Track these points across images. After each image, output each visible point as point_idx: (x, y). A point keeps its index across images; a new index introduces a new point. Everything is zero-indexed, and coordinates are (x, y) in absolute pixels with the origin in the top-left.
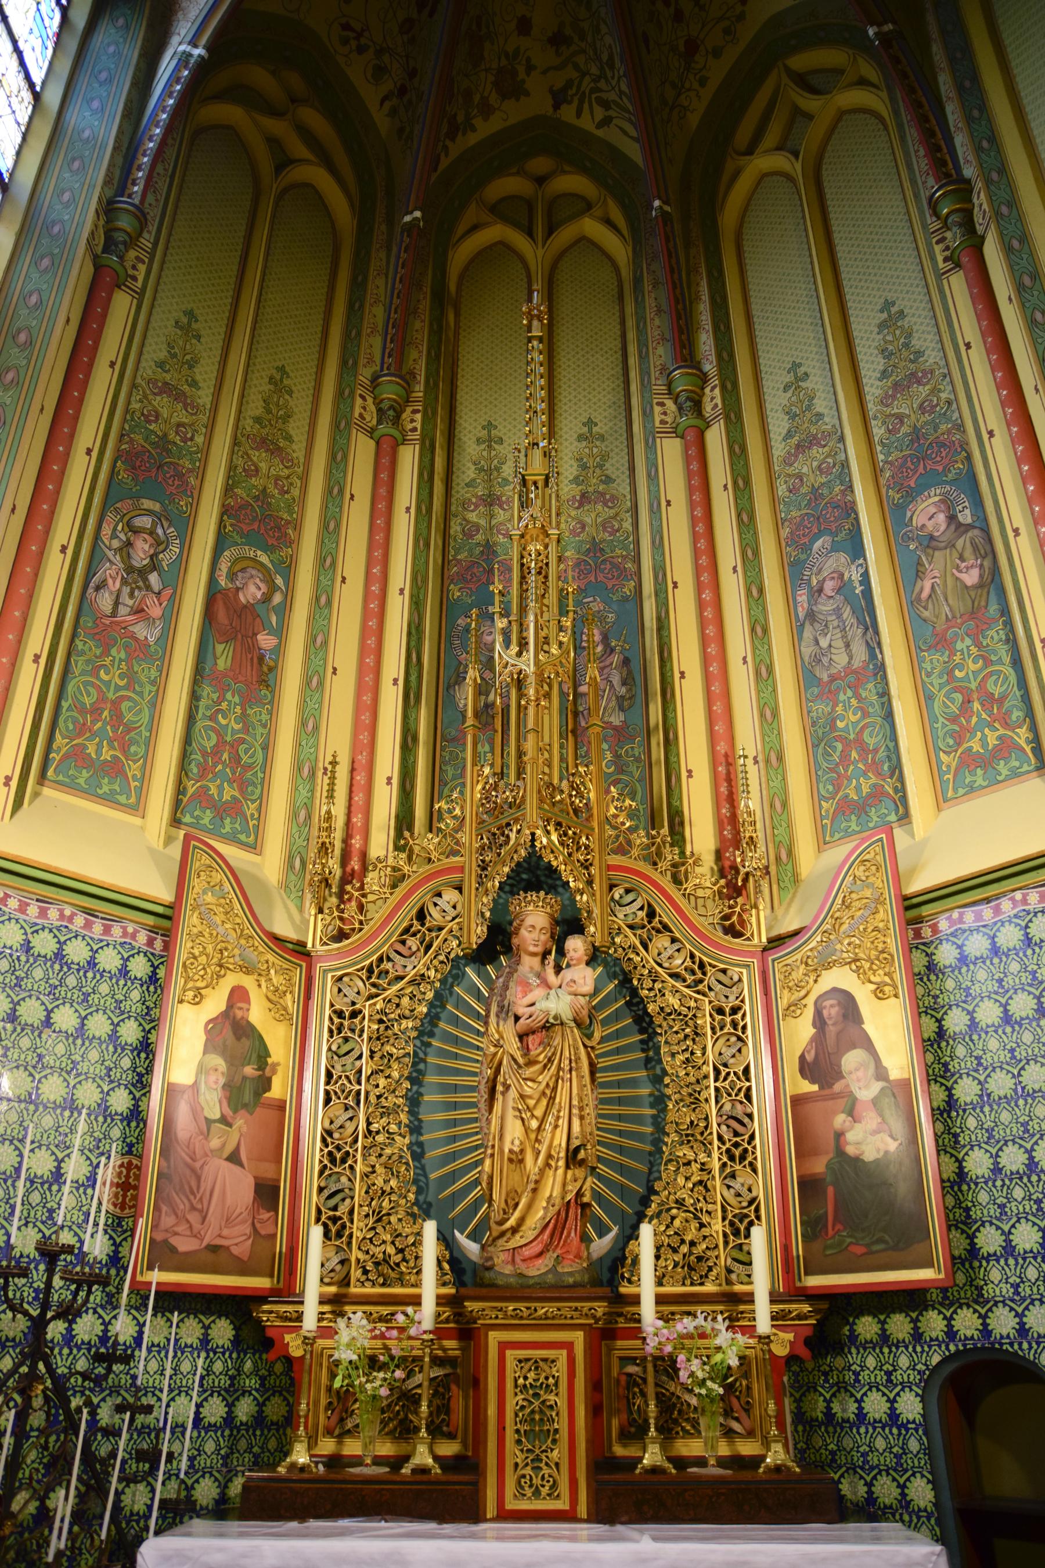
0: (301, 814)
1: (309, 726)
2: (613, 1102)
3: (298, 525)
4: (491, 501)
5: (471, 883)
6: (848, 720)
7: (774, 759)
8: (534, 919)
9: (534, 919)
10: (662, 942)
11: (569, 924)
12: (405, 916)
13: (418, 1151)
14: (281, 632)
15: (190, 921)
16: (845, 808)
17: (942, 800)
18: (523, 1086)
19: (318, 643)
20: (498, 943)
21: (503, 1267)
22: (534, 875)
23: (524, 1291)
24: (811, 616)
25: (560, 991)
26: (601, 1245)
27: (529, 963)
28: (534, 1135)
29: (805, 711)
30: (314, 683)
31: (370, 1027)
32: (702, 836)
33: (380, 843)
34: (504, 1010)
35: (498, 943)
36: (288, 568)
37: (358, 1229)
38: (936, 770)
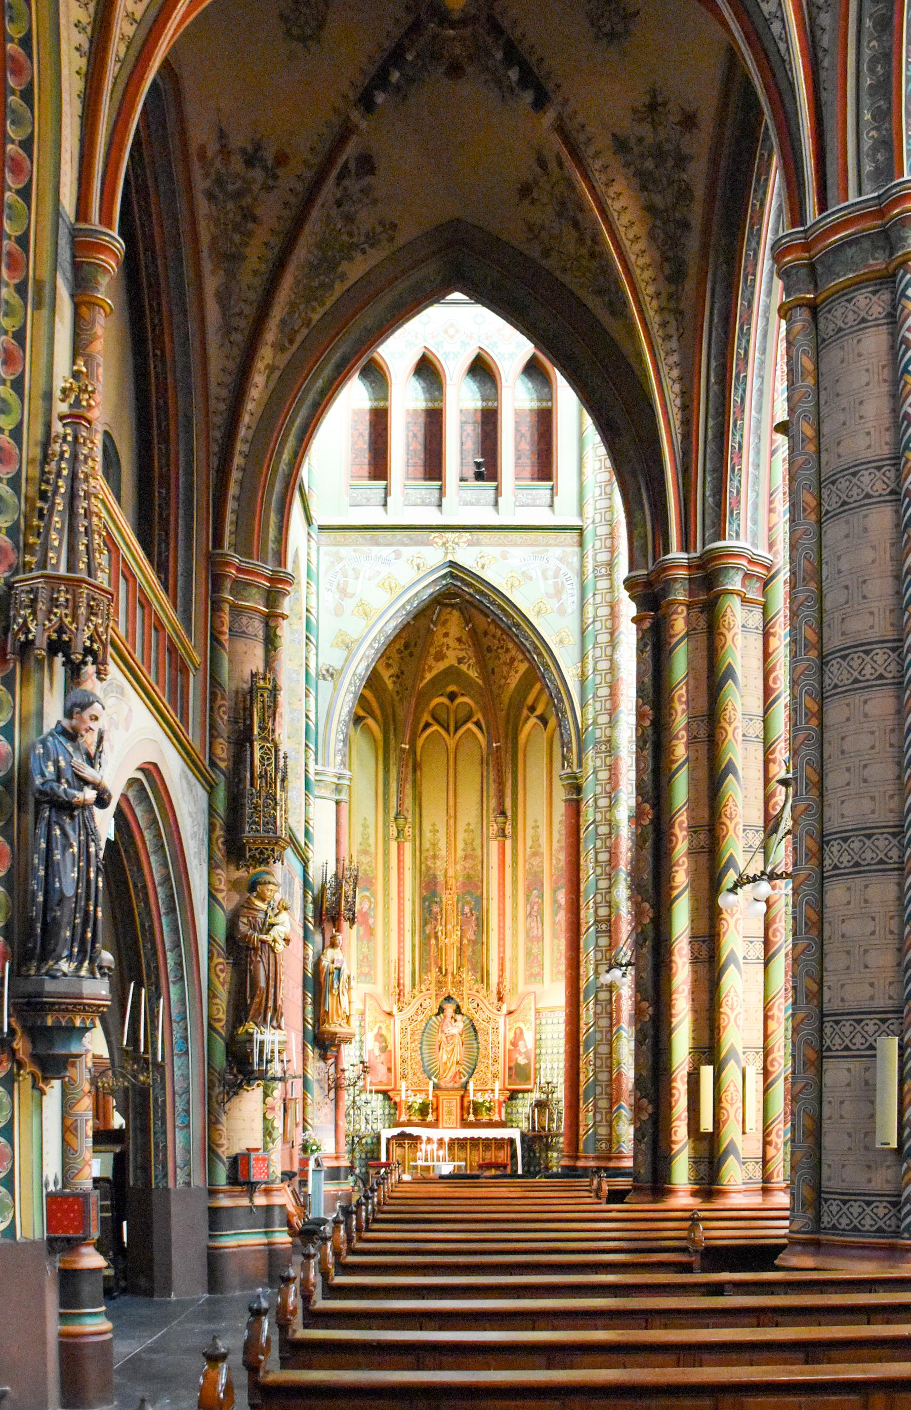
0: (387, 973)
1: (386, 949)
2: (469, 1050)
3: (375, 878)
4: (435, 857)
5: (434, 997)
6: (535, 951)
7: (515, 959)
8: (450, 1009)
9: (450, 1009)
10: (480, 1012)
11: (458, 1010)
12: (417, 1005)
13: (422, 1059)
14: (375, 917)
15: (367, 1012)
16: (531, 975)
17: (552, 981)
18: (446, 1048)
19: (386, 923)
20: (441, 1010)
21: (442, 1084)
22: (449, 999)
23: (447, 1089)
24: (530, 914)
25: (456, 1027)
26: (464, 1080)
27: (448, 1019)
28: (450, 1057)
29: (526, 944)
30: (386, 936)
31: (409, 1032)
32: (494, 979)
33: (407, 981)
34: (442, 1031)
35: (441, 1010)
36: (374, 895)
37: (410, 1076)
38: (552, 971)
